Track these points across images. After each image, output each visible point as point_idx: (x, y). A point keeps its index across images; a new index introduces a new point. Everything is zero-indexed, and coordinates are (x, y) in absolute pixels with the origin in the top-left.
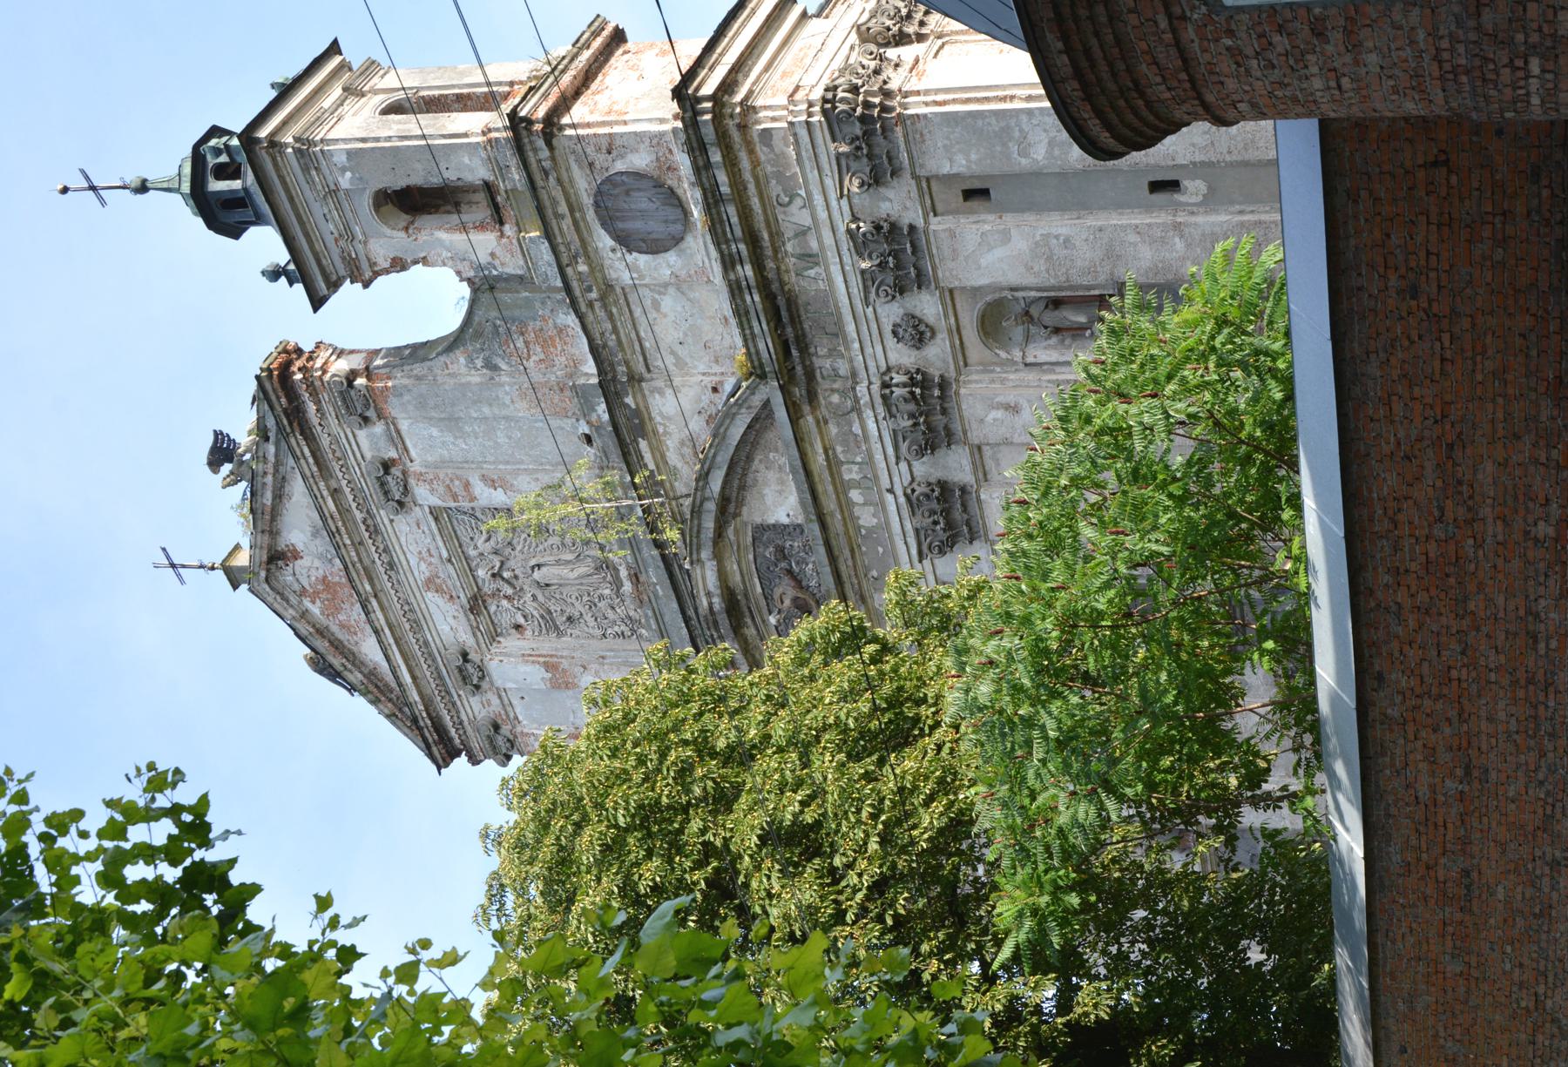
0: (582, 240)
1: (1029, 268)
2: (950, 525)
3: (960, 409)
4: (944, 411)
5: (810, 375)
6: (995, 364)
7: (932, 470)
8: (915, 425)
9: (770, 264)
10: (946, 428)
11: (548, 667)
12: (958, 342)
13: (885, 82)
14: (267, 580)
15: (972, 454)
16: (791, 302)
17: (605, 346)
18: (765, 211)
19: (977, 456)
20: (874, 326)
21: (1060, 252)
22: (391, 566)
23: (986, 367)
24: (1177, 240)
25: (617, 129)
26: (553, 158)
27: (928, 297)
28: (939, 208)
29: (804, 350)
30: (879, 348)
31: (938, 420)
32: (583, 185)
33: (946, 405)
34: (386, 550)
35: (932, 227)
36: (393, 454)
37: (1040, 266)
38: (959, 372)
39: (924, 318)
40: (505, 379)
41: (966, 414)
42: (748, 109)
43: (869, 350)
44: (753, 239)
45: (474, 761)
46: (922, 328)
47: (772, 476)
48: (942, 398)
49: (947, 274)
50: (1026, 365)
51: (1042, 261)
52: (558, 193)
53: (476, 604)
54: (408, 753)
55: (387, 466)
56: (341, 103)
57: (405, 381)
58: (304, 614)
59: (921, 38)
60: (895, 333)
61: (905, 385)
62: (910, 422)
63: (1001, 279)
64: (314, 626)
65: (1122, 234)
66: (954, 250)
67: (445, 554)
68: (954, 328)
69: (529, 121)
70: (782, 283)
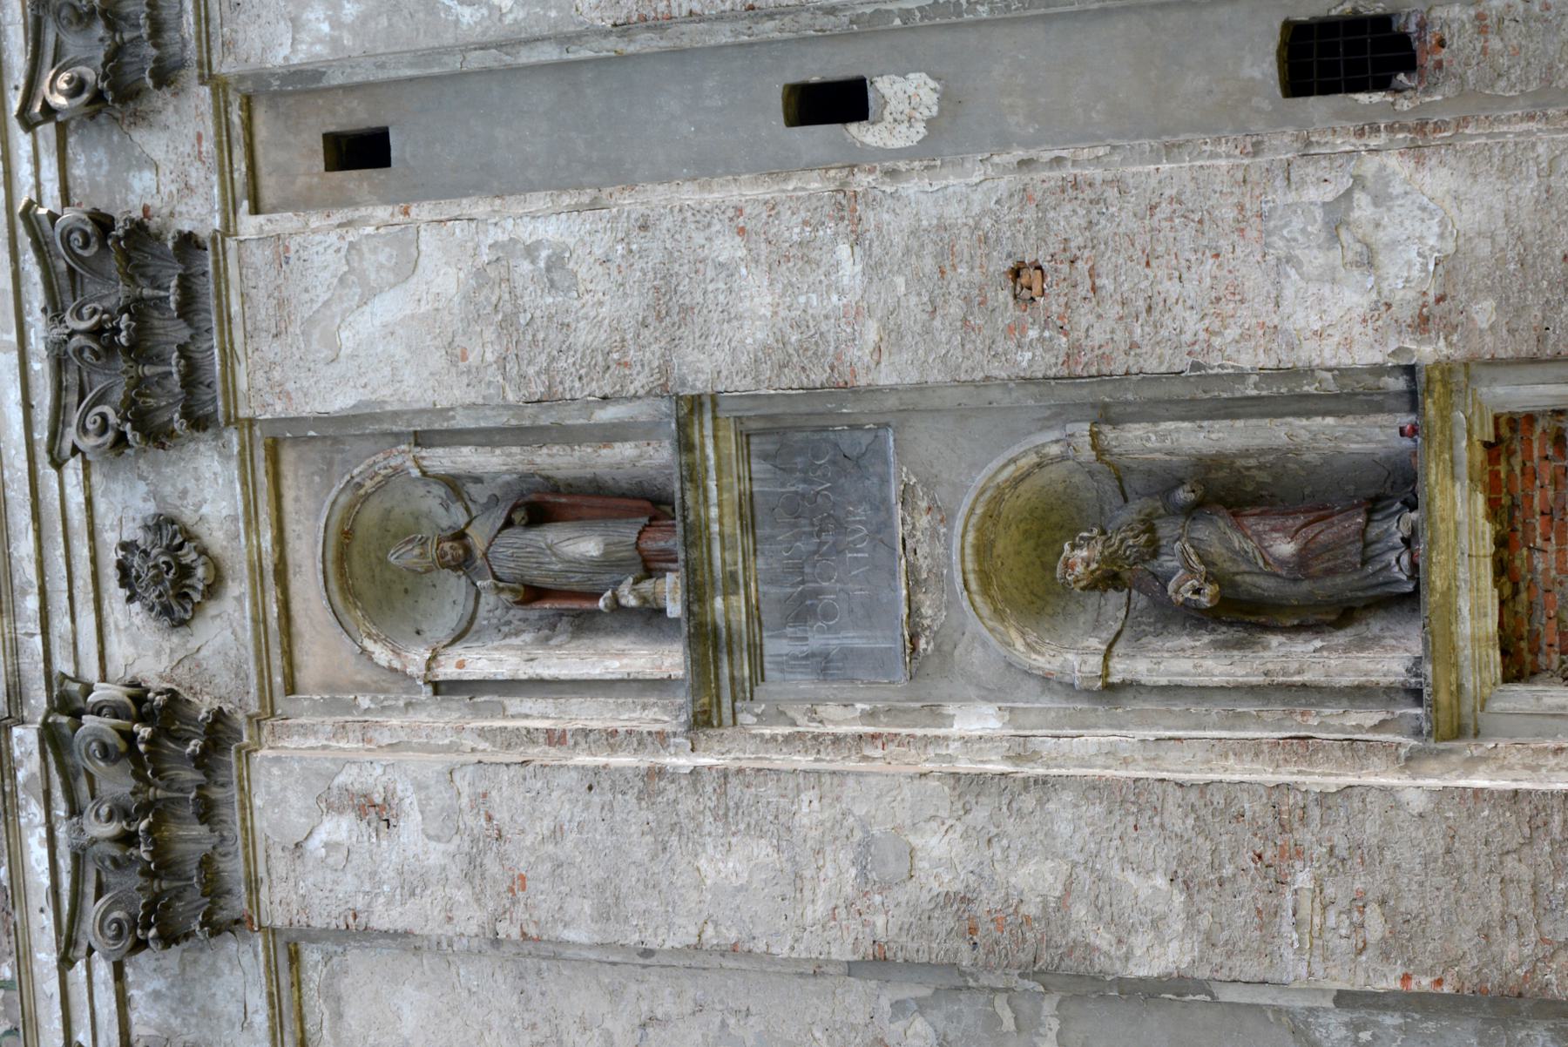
1: (456, 356)
3: (246, 807)
4: (207, 812)
6: (363, 688)
7: (175, 1022)
8: (127, 839)
10: (206, 863)
12: (273, 610)
15: (272, 970)
19: (285, 979)
20: (82, 550)
21: (540, 301)
23: (337, 699)
24: (844, 250)
27: (217, 466)
30: (87, 621)
31: (191, 837)
33: (216, 793)
37: (485, 348)
38: (269, 709)
39: (202, 530)
41: (261, 824)
43: (60, 624)
46: (189, 556)
48: (207, 761)
49: (260, 379)
50: (438, 688)
51: (489, 334)
60: (125, 575)
61: (116, 710)
62: (112, 829)
63: (385, 393)
65: (699, 238)
66: (281, 304)
68: (269, 563)
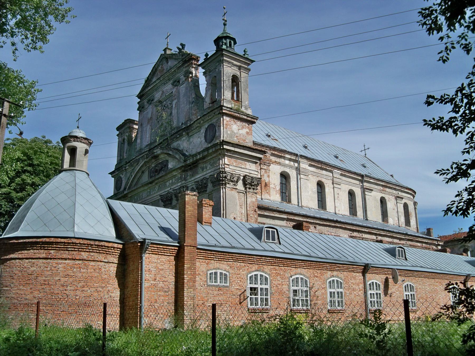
0: (206, 122)
2: (165, 201)
5: (187, 171)
9: (201, 161)
11: (151, 117)
13: (228, 183)
14: (163, 58)
16: (196, 166)
17: (192, 127)
18: (208, 160)
22: (165, 84)
25: (222, 128)
26: (217, 115)
28: (210, 196)
29: (191, 169)
32: (214, 121)
34: (167, 83)
35: (206, 195)
36: (181, 83)
40: (190, 106)
42: (224, 156)
44: (204, 158)
45: (138, 103)
47: (174, 164)
52: (212, 116)
53: (160, 102)
54: (138, 90)
55: (179, 82)
56: (236, 66)
57: (190, 85)
58: (159, 66)
59: (246, 188)
64: (157, 68)
67: (167, 95)
69: (222, 109)
70: (199, 164)
